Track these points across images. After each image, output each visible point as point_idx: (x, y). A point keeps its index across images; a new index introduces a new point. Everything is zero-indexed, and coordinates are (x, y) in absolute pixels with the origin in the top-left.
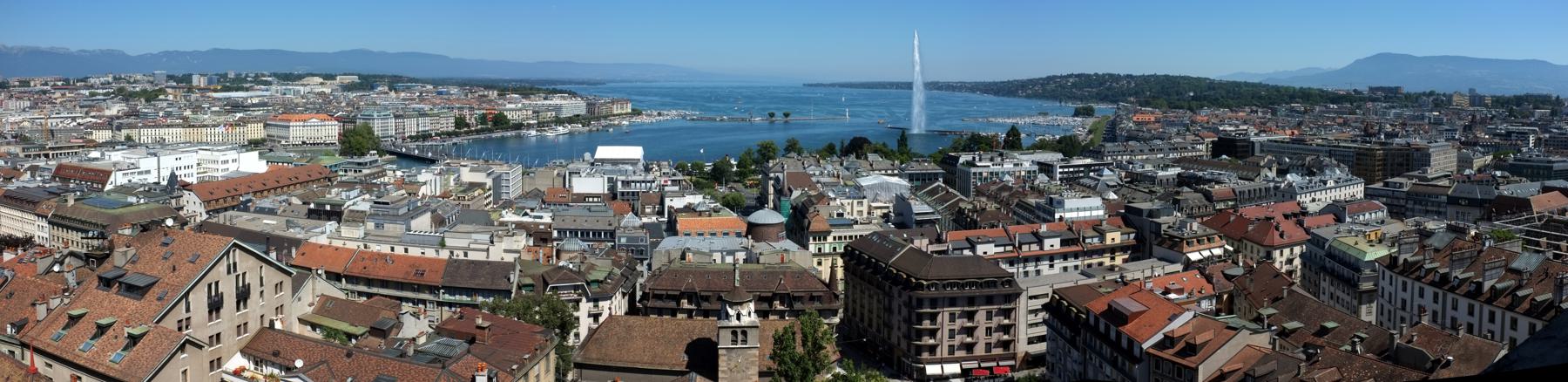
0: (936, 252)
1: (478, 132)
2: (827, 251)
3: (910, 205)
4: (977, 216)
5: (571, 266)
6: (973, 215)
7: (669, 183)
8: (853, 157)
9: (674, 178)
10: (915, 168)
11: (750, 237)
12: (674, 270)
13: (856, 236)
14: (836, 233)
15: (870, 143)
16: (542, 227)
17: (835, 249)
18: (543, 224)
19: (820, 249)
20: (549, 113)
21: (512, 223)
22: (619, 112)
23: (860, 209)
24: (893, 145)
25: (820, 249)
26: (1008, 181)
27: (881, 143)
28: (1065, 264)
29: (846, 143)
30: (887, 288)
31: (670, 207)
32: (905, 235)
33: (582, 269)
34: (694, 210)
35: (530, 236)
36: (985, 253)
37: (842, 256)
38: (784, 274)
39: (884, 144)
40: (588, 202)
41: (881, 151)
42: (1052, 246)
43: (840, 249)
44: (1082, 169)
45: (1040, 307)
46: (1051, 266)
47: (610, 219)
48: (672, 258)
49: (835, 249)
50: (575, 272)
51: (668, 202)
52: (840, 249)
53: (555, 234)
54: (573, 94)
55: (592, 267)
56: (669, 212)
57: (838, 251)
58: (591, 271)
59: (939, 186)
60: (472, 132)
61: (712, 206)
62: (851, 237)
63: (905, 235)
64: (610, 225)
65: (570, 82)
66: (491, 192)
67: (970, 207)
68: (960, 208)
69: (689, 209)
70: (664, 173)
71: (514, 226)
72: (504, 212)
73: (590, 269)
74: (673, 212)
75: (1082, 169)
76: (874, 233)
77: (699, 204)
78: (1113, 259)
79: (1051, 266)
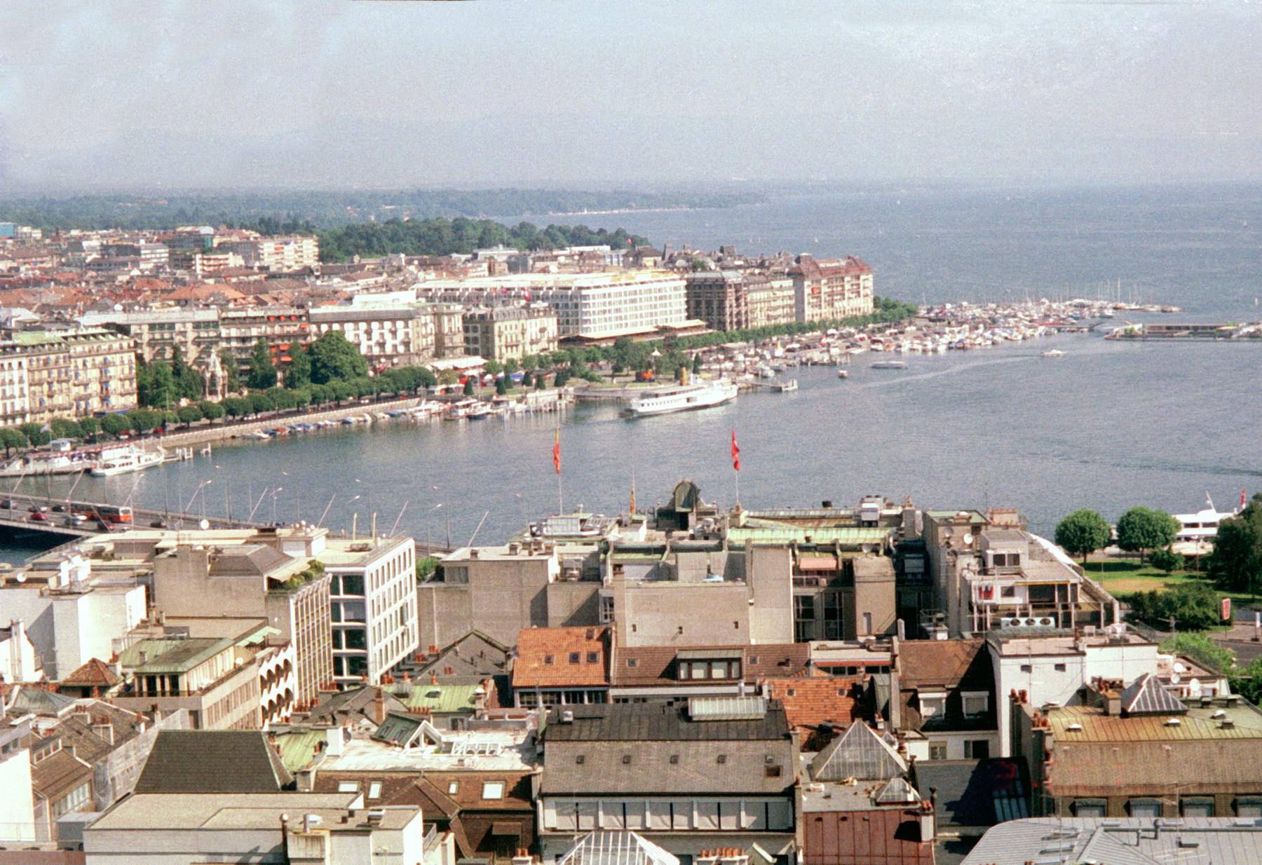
1: (233, 411)
16: (493, 792)
18: (495, 776)
20: (532, 327)
21: (363, 779)
22: (826, 311)
35: (444, 826)
40: (690, 681)
51: (1009, 678)
56: (1017, 713)
60: (208, 412)
64: (775, 772)
65: (622, 198)
66: (290, 654)
70: (999, 560)
71: (375, 791)
72: (334, 736)
77: (1138, 685)
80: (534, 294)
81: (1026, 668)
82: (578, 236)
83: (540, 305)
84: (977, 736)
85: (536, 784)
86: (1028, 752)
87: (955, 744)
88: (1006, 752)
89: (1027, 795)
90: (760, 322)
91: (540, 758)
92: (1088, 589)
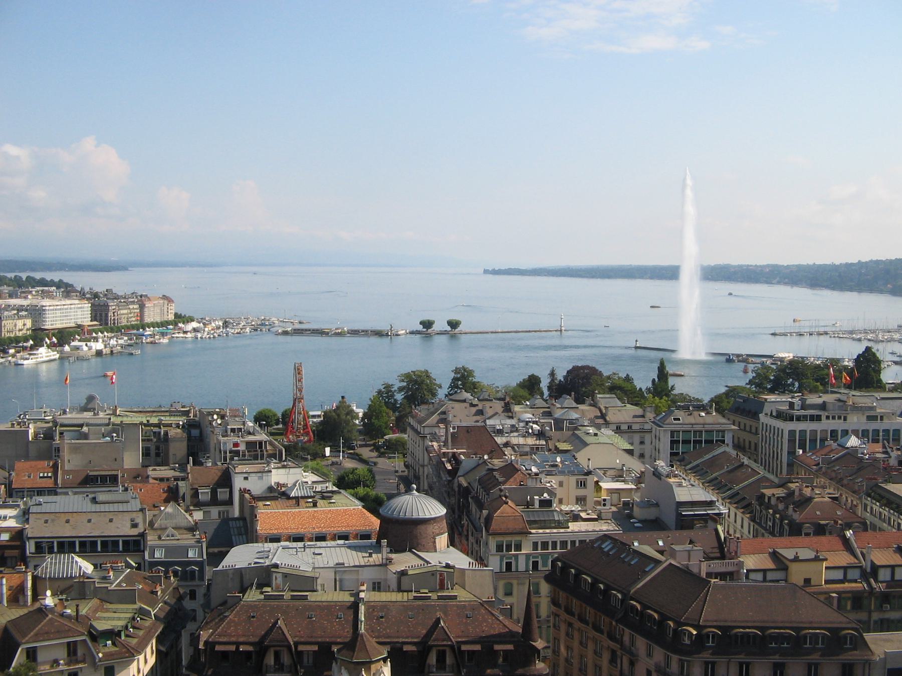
3: (670, 487)
6: (787, 508)
7: (242, 447)
8: (569, 401)
9: (251, 438)
10: (684, 421)
11: (384, 542)
13: (573, 542)
14: (538, 533)
15: (600, 374)
17: (535, 564)
19: (509, 565)
20: (20, 323)
23: (581, 492)
24: (643, 381)
25: (509, 565)
26: (855, 450)
27: (624, 376)
29: (560, 375)
30: (626, 639)
31: (243, 492)
32: (661, 543)
34: (285, 495)
37: (549, 578)
39: (628, 379)
41: (620, 388)
43: (544, 565)
47: (134, 515)
49: (535, 564)
51: (239, 483)
52: (544, 565)
53: (30, 547)
54: (68, 290)
56: (242, 497)
57: (540, 567)
61: (319, 488)
62: (564, 544)
63: (661, 543)
64: (135, 526)
67: (780, 492)
68: (763, 495)
69: (278, 494)
70: (233, 430)
74: (250, 502)
76: (606, 537)
77: (295, 485)
80: (20, 309)
81: (246, 478)
82: (43, 283)
83: (24, 313)
84: (222, 508)
85: (25, 532)
86: (247, 515)
87: (214, 511)
88: (237, 514)
89: (246, 533)
90: (124, 322)
91: (27, 521)
92: (271, 443)
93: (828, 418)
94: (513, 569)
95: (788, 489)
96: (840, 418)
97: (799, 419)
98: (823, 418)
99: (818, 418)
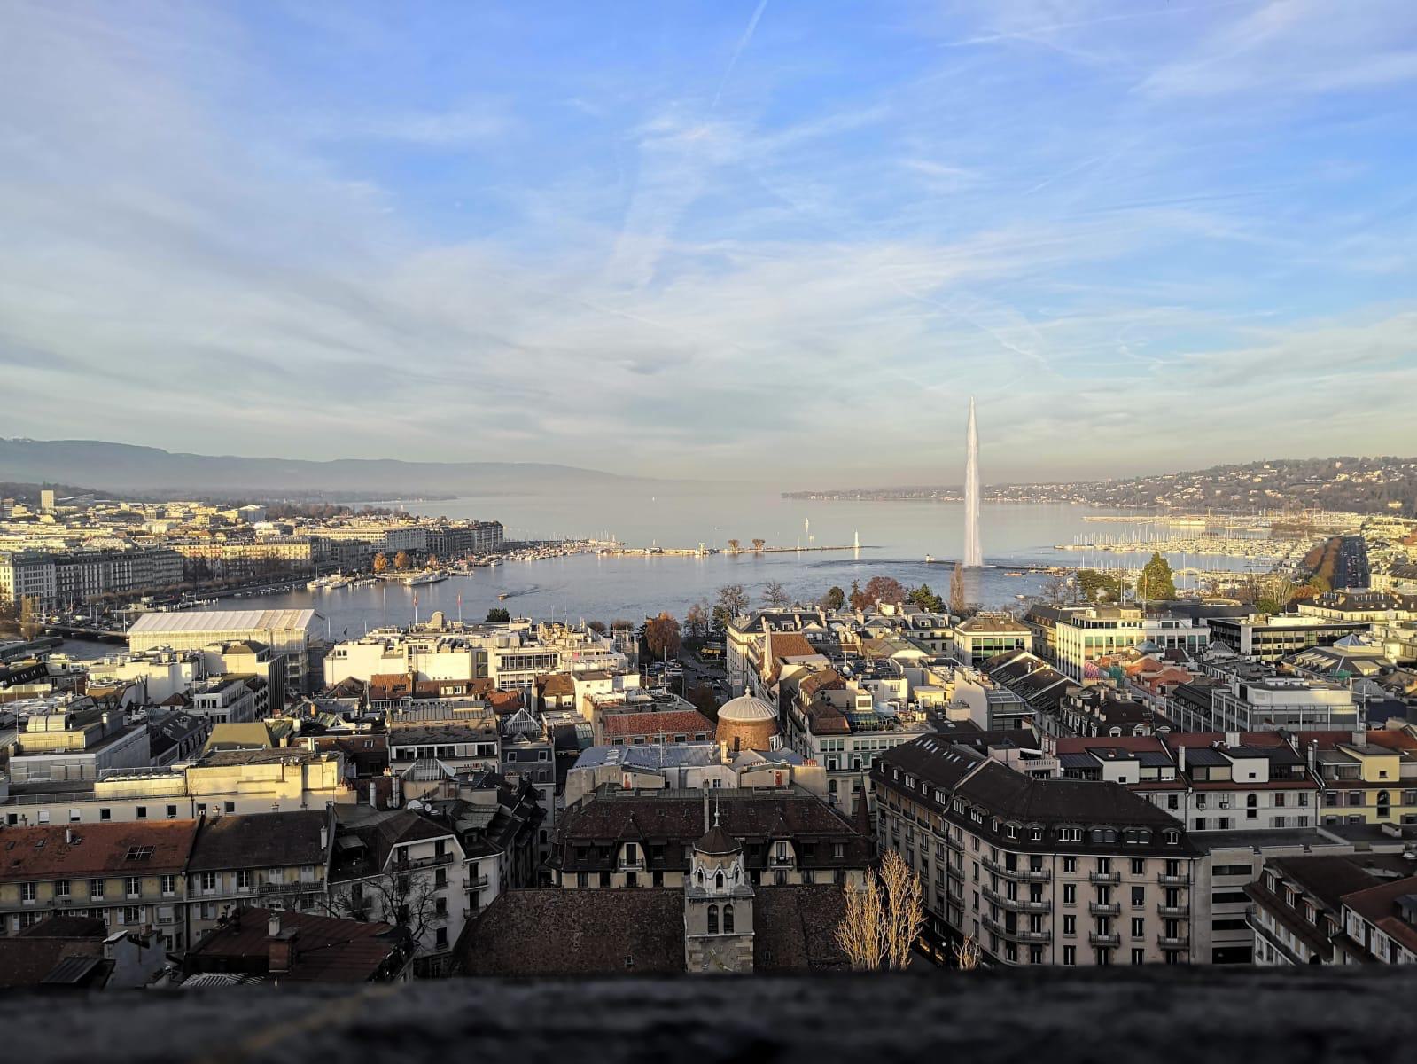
0: (1035, 772)
2: (845, 766)
4: (1100, 712)
5: (428, 808)
12: (603, 804)
17: (857, 762)
28: (1280, 812)
33: (448, 813)
36: (1122, 779)
38: (783, 802)
42: (1252, 775)
44: (1302, 634)
45: (1240, 890)
46: (1252, 814)
48: (598, 783)
49: (857, 762)
50: (435, 818)
55: (465, 806)
58: (465, 815)
59: (1027, 659)
73: (460, 812)
75: (1302, 634)
78: (1383, 812)
79: (1252, 814)
93: (1123, 625)
94: (837, 767)
95: (1094, 692)
96: (1135, 625)
97: (1095, 626)
98: (1119, 625)
99: (1114, 626)
